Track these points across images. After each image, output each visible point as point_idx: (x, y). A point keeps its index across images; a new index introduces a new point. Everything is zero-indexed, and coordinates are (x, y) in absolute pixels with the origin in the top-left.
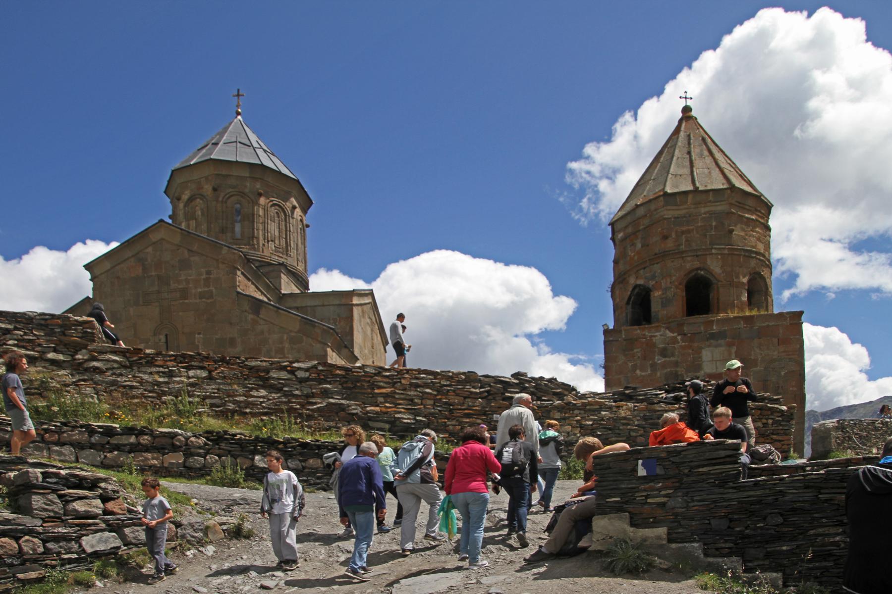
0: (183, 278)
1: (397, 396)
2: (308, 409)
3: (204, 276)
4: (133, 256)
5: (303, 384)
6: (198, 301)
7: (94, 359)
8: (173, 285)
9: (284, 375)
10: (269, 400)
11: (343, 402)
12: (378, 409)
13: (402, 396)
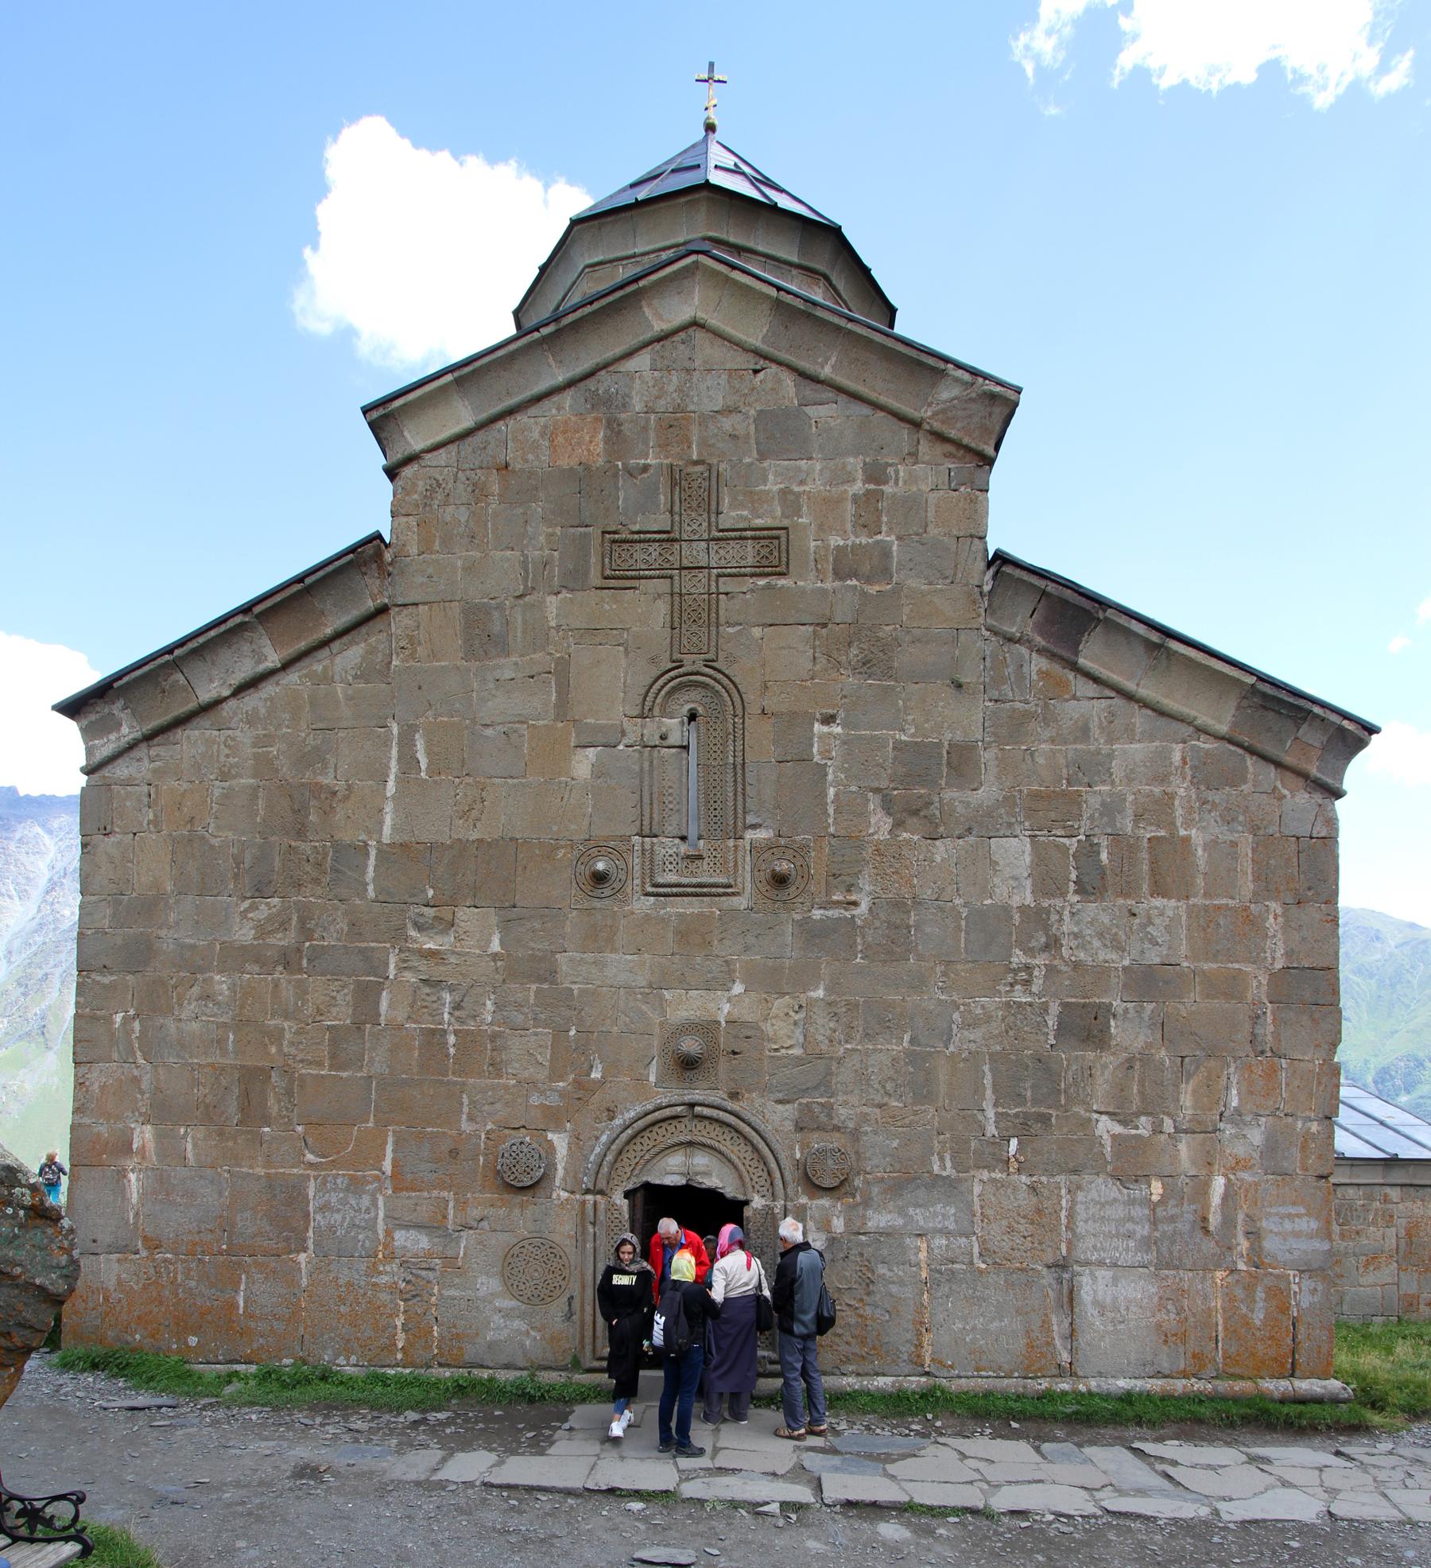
0: (773, 485)
3: (858, 487)
4: (570, 384)
6: (837, 584)
8: (732, 515)
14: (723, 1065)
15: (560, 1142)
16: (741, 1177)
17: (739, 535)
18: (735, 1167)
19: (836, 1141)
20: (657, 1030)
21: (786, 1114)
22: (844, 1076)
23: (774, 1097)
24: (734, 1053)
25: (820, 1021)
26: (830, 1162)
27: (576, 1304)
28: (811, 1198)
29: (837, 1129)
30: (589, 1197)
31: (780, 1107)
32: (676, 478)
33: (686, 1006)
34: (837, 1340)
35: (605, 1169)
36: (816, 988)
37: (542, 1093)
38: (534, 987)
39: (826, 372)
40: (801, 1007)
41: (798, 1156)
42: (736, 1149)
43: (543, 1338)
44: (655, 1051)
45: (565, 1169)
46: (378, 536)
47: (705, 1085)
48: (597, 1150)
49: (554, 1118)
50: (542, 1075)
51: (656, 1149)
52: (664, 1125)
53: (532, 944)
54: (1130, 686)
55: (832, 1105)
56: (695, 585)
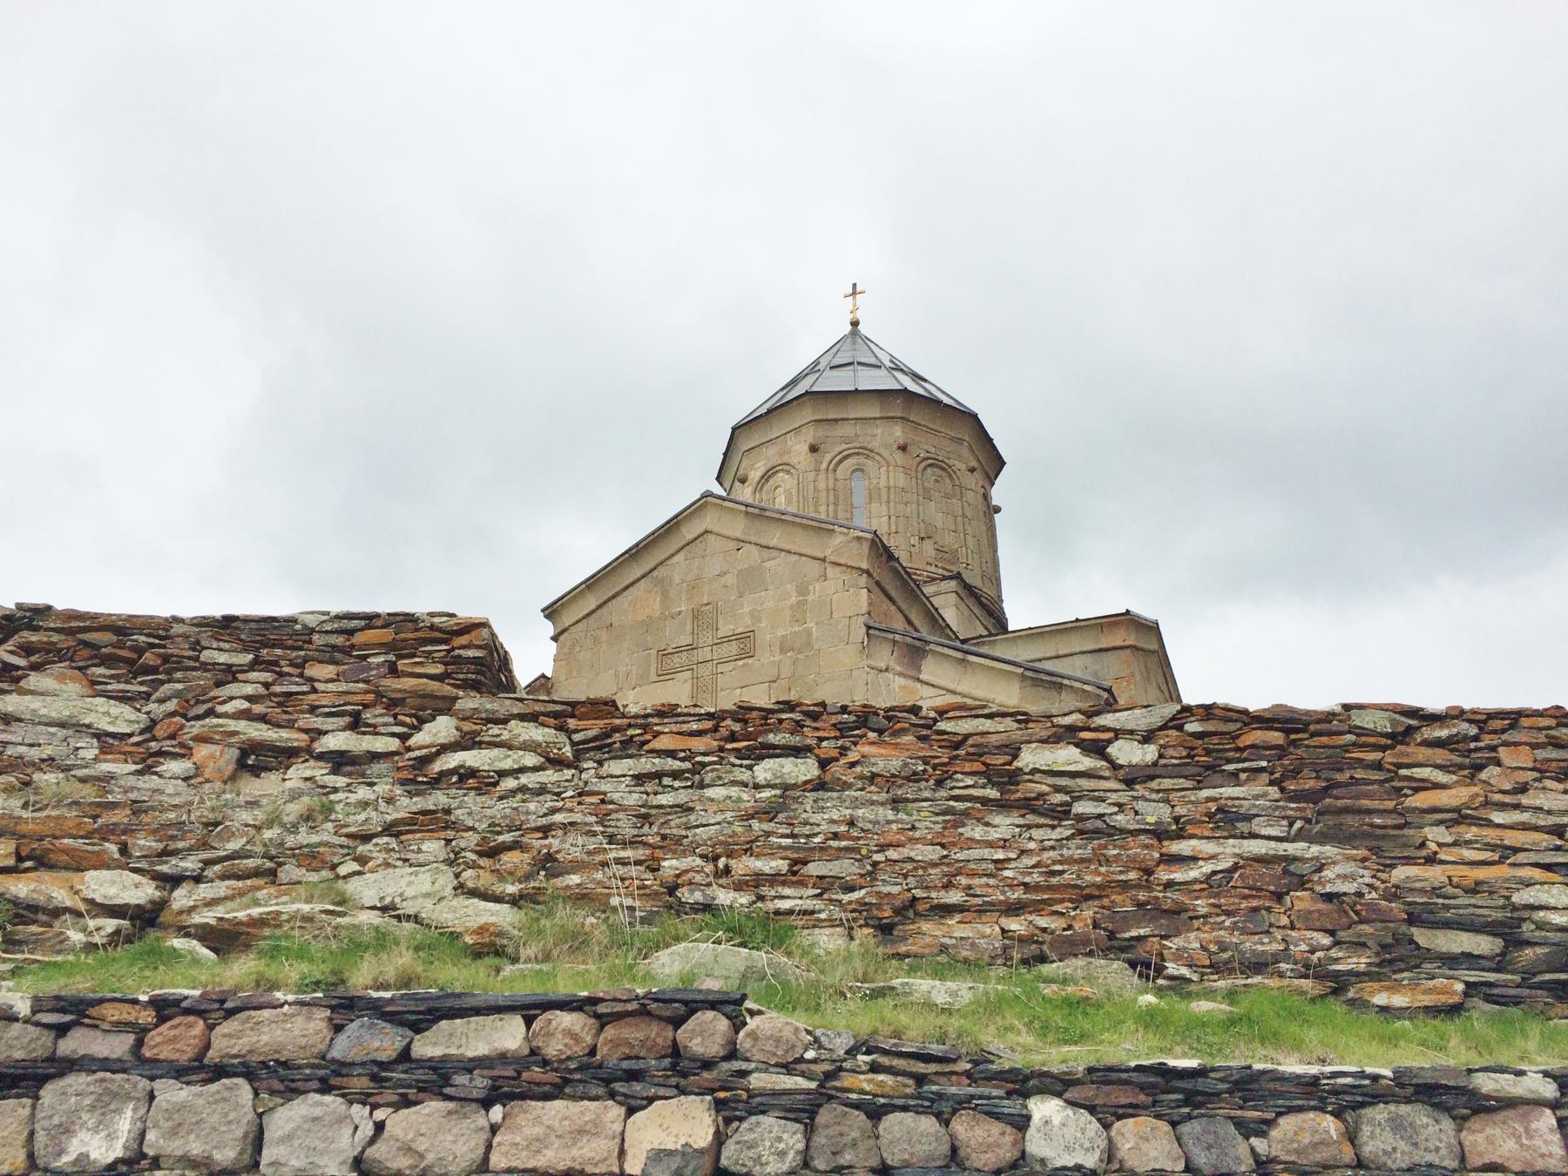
1: (1498, 817)
2: (1169, 885)
3: (793, 600)
4: (643, 576)
5: (1140, 790)
7: (467, 742)
9: (1068, 757)
10: (1023, 852)
11: (1293, 848)
12: (1436, 874)
13: (1524, 817)
17: (728, 639)
32: (696, 615)
39: (774, 542)
46: (543, 676)
54: (952, 686)
56: (705, 671)
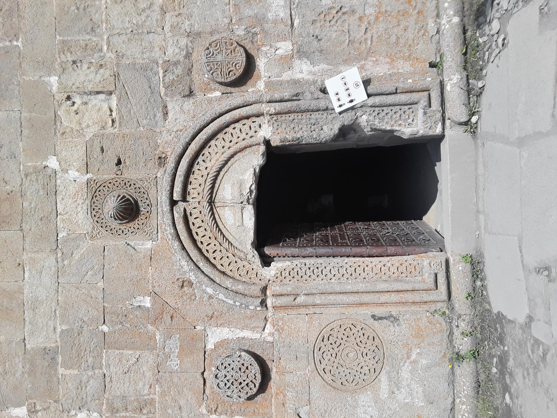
14: (130, 174)
15: (216, 336)
16: (241, 150)
18: (232, 156)
19: (199, 57)
20: (99, 243)
21: (178, 108)
22: (134, 52)
23: (161, 123)
24: (119, 163)
25: (82, 78)
26: (219, 58)
27: (379, 311)
28: (259, 78)
29: (188, 55)
30: (269, 302)
31: (170, 115)
33: (74, 212)
34: (402, 41)
35: (240, 287)
36: (49, 84)
37: (167, 357)
38: (61, 371)
40: (68, 98)
41: (218, 94)
42: (215, 157)
43: (418, 346)
44: (120, 242)
45: (242, 329)
47: (152, 192)
48: (221, 296)
49: (193, 343)
50: (149, 358)
51: (219, 235)
52: (194, 229)
53: (18, 374)
55: (165, 62)
